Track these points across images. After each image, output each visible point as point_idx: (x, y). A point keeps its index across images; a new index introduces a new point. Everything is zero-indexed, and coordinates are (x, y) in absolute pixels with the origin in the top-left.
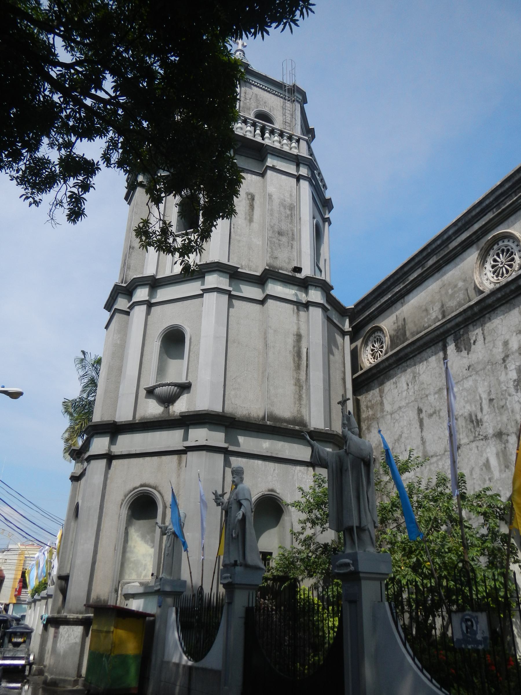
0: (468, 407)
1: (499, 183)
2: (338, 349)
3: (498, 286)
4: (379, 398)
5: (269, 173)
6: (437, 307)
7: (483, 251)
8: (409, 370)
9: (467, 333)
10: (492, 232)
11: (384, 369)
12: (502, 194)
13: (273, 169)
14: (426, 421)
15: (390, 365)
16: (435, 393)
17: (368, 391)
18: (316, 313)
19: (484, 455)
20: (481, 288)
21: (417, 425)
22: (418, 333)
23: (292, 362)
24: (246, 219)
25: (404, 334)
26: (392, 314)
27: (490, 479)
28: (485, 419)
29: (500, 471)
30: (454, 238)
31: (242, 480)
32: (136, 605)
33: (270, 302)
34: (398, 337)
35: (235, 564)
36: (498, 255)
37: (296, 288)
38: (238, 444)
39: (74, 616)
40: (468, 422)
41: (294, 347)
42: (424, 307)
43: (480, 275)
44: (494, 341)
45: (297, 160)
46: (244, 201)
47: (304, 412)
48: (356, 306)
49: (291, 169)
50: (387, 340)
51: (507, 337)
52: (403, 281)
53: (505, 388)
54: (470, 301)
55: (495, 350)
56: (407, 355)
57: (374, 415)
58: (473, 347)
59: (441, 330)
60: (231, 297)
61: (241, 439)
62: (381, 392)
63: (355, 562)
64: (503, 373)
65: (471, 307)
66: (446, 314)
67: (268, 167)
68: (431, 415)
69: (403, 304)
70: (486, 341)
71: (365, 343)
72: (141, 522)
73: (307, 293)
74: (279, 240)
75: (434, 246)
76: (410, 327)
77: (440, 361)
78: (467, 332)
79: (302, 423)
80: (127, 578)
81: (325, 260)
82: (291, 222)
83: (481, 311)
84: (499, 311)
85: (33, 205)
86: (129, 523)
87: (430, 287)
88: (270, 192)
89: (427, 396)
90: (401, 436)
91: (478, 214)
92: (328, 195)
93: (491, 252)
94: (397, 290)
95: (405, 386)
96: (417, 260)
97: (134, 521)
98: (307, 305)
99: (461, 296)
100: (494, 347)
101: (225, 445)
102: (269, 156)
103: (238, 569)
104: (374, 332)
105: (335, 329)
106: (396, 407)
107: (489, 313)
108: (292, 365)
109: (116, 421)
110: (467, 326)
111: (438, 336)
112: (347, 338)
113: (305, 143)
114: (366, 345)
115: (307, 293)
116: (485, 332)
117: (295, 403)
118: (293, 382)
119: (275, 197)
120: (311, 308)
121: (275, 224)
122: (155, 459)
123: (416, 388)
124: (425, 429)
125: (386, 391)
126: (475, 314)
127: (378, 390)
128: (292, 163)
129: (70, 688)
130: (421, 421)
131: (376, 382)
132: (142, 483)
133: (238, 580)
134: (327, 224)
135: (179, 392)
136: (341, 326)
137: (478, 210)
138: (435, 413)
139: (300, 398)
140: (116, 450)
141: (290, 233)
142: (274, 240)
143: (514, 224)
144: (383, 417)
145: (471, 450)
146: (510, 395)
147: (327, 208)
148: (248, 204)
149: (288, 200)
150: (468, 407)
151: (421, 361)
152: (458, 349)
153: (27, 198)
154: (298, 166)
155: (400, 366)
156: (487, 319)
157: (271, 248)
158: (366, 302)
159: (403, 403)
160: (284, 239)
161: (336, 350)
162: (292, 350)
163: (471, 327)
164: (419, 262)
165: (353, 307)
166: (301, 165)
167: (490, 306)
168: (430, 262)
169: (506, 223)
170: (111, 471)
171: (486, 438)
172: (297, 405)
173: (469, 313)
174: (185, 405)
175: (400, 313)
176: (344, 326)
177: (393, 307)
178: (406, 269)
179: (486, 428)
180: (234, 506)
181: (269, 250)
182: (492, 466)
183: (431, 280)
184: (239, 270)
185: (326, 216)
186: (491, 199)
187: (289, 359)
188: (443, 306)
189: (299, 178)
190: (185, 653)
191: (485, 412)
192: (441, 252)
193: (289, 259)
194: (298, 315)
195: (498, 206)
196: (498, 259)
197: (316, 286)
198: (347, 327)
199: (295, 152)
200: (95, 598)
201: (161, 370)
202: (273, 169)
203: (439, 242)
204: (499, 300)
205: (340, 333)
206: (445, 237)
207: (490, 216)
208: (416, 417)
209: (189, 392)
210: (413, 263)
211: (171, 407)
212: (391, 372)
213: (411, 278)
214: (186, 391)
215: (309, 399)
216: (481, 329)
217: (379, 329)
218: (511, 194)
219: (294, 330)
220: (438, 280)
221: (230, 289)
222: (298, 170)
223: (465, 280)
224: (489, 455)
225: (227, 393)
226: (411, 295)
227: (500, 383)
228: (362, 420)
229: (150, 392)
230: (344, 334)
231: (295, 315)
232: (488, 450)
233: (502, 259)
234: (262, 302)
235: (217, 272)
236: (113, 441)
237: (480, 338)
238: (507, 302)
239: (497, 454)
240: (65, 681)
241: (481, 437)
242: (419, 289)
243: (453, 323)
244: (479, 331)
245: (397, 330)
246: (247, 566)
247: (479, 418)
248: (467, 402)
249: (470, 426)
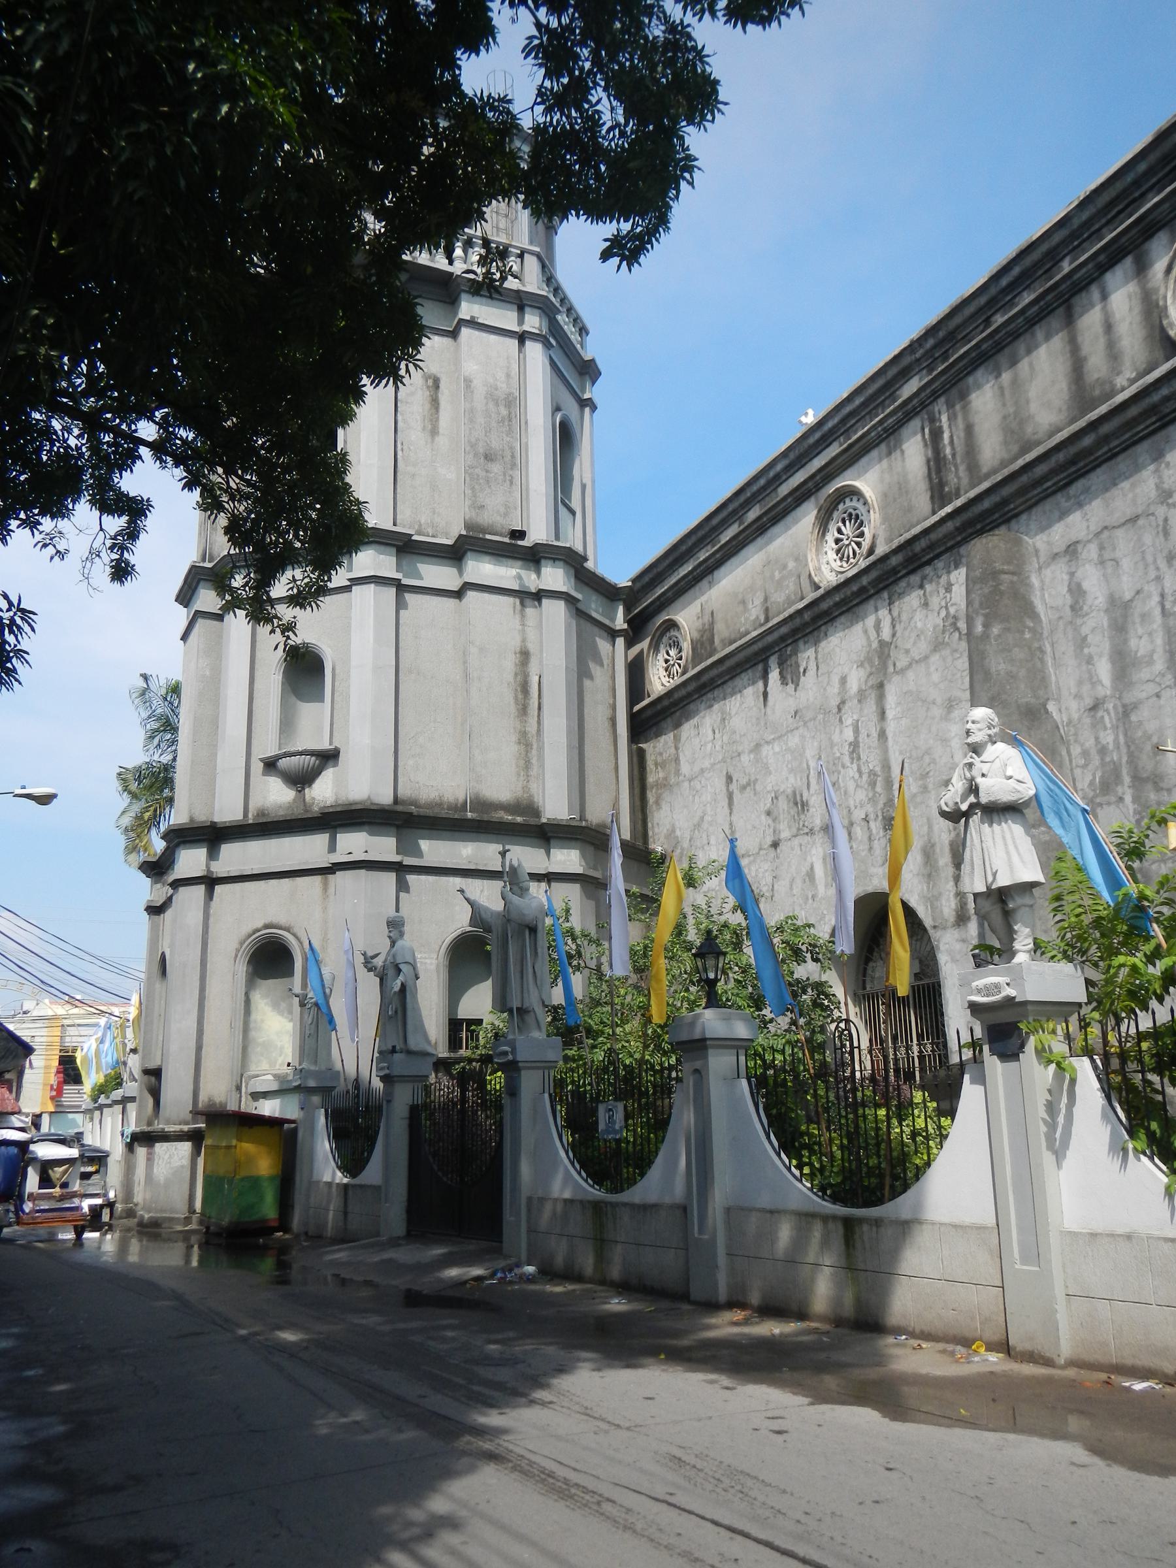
0: (792, 780)
1: (845, 395)
2: (602, 665)
3: (842, 578)
4: (673, 750)
5: (465, 332)
6: (758, 601)
7: (823, 512)
8: (716, 707)
9: (796, 654)
10: (833, 482)
11: (682, 699)
12: (851, 414)
13: (473, 323)
14: (737, 797)
15: (689, 695)
16: (751, 752)
17: (658, 735)
18: (556, 610)
19: (809, 858)
20: (816, 579)
21: (725, 803)
22: (731, 643)
23: (512, 701)
24: (424, 429)
25: (711, 640)
26: (696, 599)
27: (813, 897)
28: (811, 802)
29: (826, 886)
30: (784, 477)
31: (402, 934)
32: (269, 1108)
33: (471, 595)
34: (702, 644)
35: (393, 1050)
36: (844, 522)
37: (519, 563)
38: (419, 853)
39: (177, 1128)
40: (791, 804)
41: (516, 674)
42: (740, 596)
43: (817, 555)
44: (829, 673)
46: (420, 392)
47: (534, 787)
48: (634, 581)
49: (506, 318)
50: (686, 646)
51: (846, 670)
52: (712, 542)
53: (838, 755)
54: (802, 598)
55: (828, 688)
56: (712, 680)
57: (665, 779)
58: (802, 679)
59: (760, 645)
60: (401, 588)
61: (424, 845)
62: (677, 739)
63: (514, 1051)
64: (837, 730)
65: (799, 612)
66: (770, 615)
67: (462, 322)
68: (743, 788)
69: (711, 584)
70: (820, 671)
71: (655, 647)
72: (271, 983)
73: (538, 573)
74: (487, 471)
75: (755, 488)
76: (722, 631)
77: (758, 697)
78: (795, 652)
79: (530, 808)
80: (253, 1069)
81: (584, 487)
82: (510, 432)
83: (815, 619)
84: (837, 623)
85: (56, 558)
86: (250, 985)
87: (750, 562)
88: (467, 374)
89: (739, 755)
90: (702, 818)
91: (818, 442)
92: (591, 350)
93: (836, 515)
94: (703, 555)
95: (710, 732)
96: (731, 508)
97: (260, 981)
98: (539, 596)
99: (791, 586)
100: (828, 683)
101: (397, 858)
102: (464, 296)
103: (397, 1056)
104: (668, 629)
105: (596, 630)
106: (696, 769)
107: (825, 623)
108: (513, 709)
109: (216, 820)
110: (796, 641)
111: (756, 654)
112: (620, 642)
113: (535, 259)
114: (657, 650)
115: (538, 573)
116: (819, 656)
117: (519, 775)
118: (514, 738)
119: (477, 383)
120: (545, 601)
121: (478, 440)
122: (286, 882)
123: (725, 738)
124: (735, 811)
125: (683, 738)
126: (805, 625)
127: (671, 735)
128: (509, 306)
129: (179, 1228)
130: (730, 797)
131: (669, 720)
132: (268, 920)
133: (396, 1072)
134: (587, 410)
135: (319, 765)
136: (607, 622)
137: (818, 435)
138: (748, 784)
139: (527, 765)
140: (220, 868)
141: (508, 454)
142: (478, 471)
143: (866, 472)
144: (678, 784)
145: (792, 849)
146: (843, 766)
147: (587, 377)
148: (429, 399)
150: (792, 780)
151: (733, 694)
152: (784, 681)
153: (45, 546)
154: (521, 309)
155: (704, 698)
156: (822, 634)
157: (473, 489)
158: (655, 571)
159: (707, 764)
160: (496, 468)
161: (598, 668)
162: (511, 678)
163: (801, 643)
164: (735, 512)
165: (630, 584)
166: (527, 309)
167: (826, 613)
168: (752, 515)
169: (849, 473)
170: (213, 904)
171: (811, 832)
172: (522, 778)
173: (798, 622)
174: (330, 785)
175: (707, 602)
176: (613, 619)
177: (697, 588)
178: (715, 521)
179: (812, 816)
180: (391, 972)
181: (469, 492)
182: (817, 877)
183: (751, 548)
184: (415, 538)
185: (586, 396)
186: (836, 420)
187: (507, 697)
188: (766, 599)
189: (522, 338)
190: (339, 1168)
191: (812, 790)
192: (767, 499)
193: (507, 507)
194: (523, 616)
195: (847, 433)
196: (843, 528)
197: (554, 560)
198: (620, 622)
200: (206, 1100)
201: (287, 724)
202: (473, 323)
203: (762, 482)
204: (837, 605)
205: (605, 634)
206: (772, 474)
207: (834, 450)
208: (724, 789)
209: (336, 765)
210: (724, 514)
211: (307, 790)
212: (692, 706)
213: (726, 537)
214: (331, 763)
215: (542, 766)
216: (813, 650)
217: (672, 625)
218: (864, 417)
219: (515, 643)
220: (761, 550)
221: (398, 576)
222: (521, 321)
223: (797, 559)
224: (814, 859)
225: (400, 764)
226: (723, 570)
227: (832, 745)
228: (648, 785)
229: (270, 765)
230: (613, 634)
231: (518, 616)
232: (814, 851)
233: (848, 530)
234: (458, 594)
235: (374, 546)
236: (213, 854)
237: (812, 666)
238: (848, 610)
239: (824, 859)
240: (171, 1219)
241: (806, 830)
242: (734, 561)
243: (776, 635)
244: (810, 652)
245: (702, 632)
246: (409, 1052)
247: (804, 799)
248: (791, 771)
249: (793, 811)
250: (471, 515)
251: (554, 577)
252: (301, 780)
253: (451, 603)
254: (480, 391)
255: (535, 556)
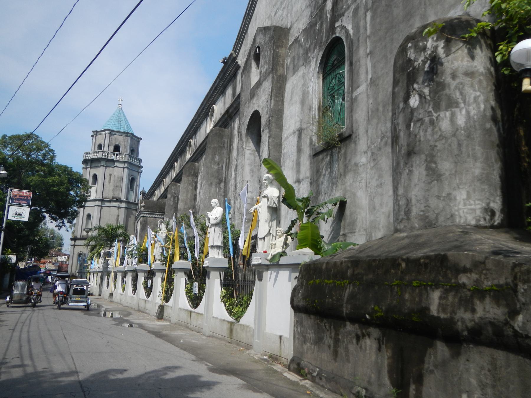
13: (116, 167)
18: (123, 210)
45: (124, 162)
49: (122, 165)
60: (101, 207)
81: (137, 186)
98: (121, 207)
149: (120, 176)
160: (118, 188)
189: (124, 168)
199: (124, 160)
201: (87, 224)
202: (116, 167)
219: (117, 214)
222: (124, 165)
229: (84, 229)
236: (75, 242)
250: (113, 195)
251: (123, 205)
252: (87, 232)
253: (109, 208)
254: (116, 176)
255: (121, 202)
